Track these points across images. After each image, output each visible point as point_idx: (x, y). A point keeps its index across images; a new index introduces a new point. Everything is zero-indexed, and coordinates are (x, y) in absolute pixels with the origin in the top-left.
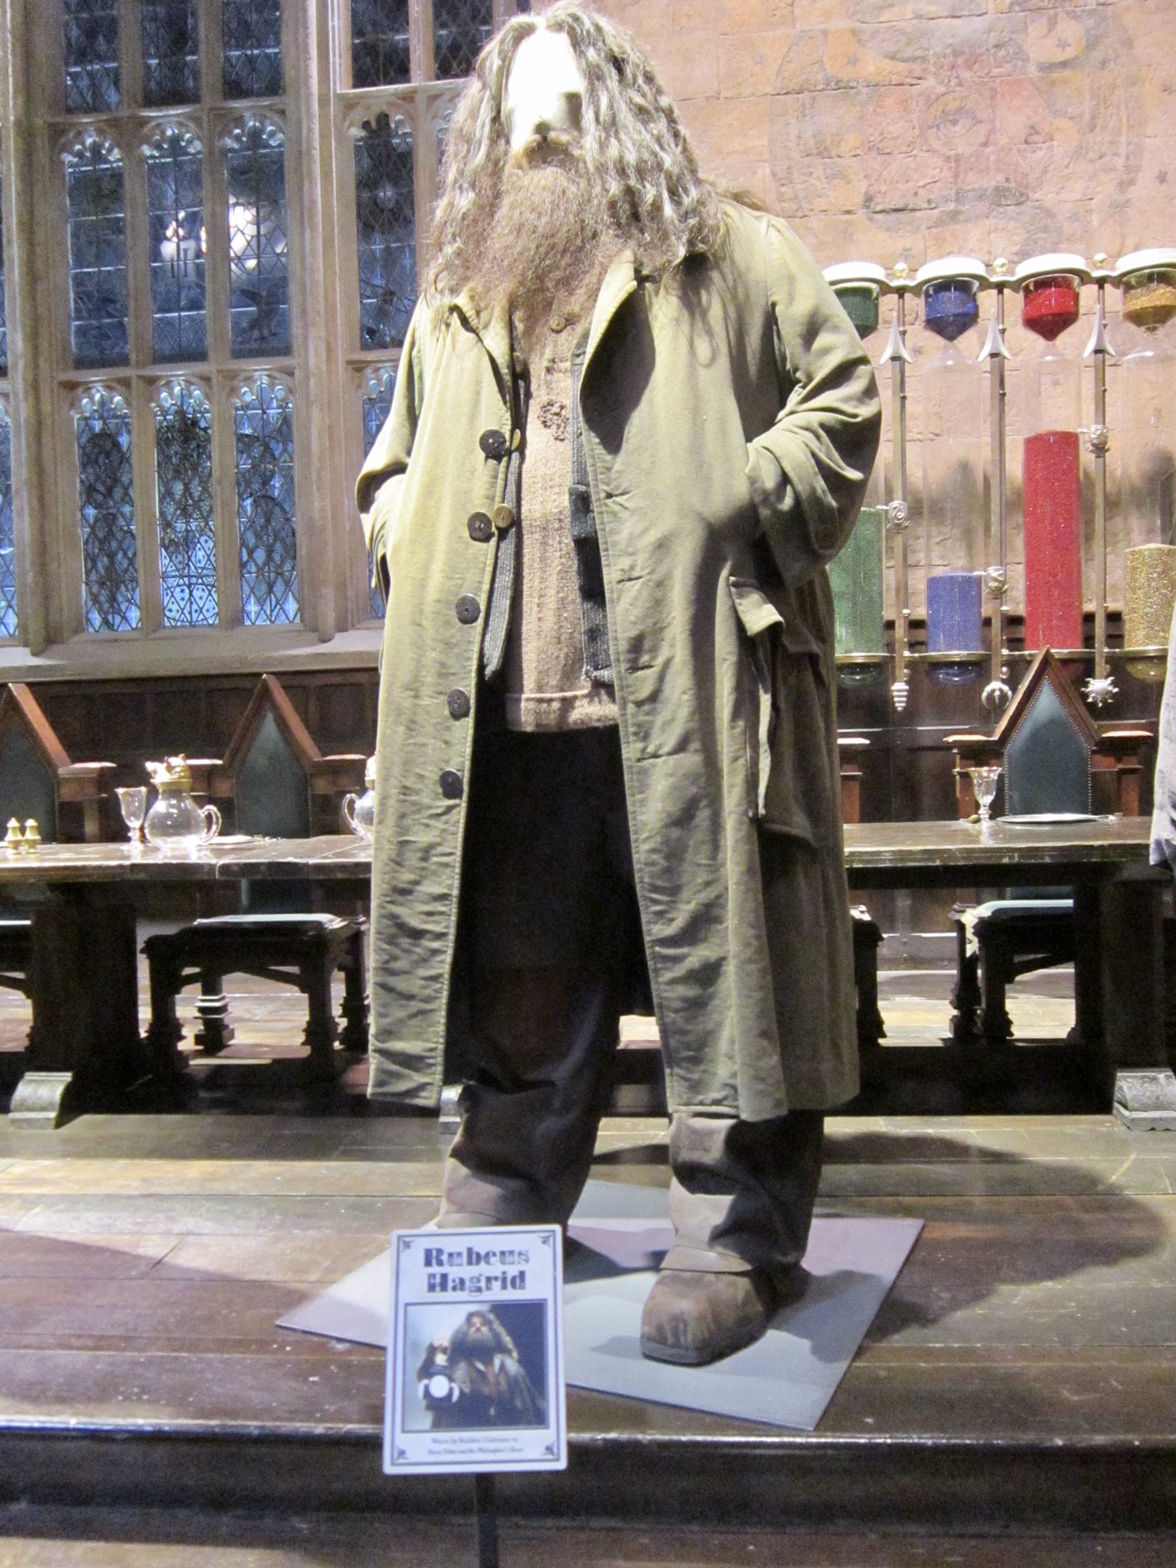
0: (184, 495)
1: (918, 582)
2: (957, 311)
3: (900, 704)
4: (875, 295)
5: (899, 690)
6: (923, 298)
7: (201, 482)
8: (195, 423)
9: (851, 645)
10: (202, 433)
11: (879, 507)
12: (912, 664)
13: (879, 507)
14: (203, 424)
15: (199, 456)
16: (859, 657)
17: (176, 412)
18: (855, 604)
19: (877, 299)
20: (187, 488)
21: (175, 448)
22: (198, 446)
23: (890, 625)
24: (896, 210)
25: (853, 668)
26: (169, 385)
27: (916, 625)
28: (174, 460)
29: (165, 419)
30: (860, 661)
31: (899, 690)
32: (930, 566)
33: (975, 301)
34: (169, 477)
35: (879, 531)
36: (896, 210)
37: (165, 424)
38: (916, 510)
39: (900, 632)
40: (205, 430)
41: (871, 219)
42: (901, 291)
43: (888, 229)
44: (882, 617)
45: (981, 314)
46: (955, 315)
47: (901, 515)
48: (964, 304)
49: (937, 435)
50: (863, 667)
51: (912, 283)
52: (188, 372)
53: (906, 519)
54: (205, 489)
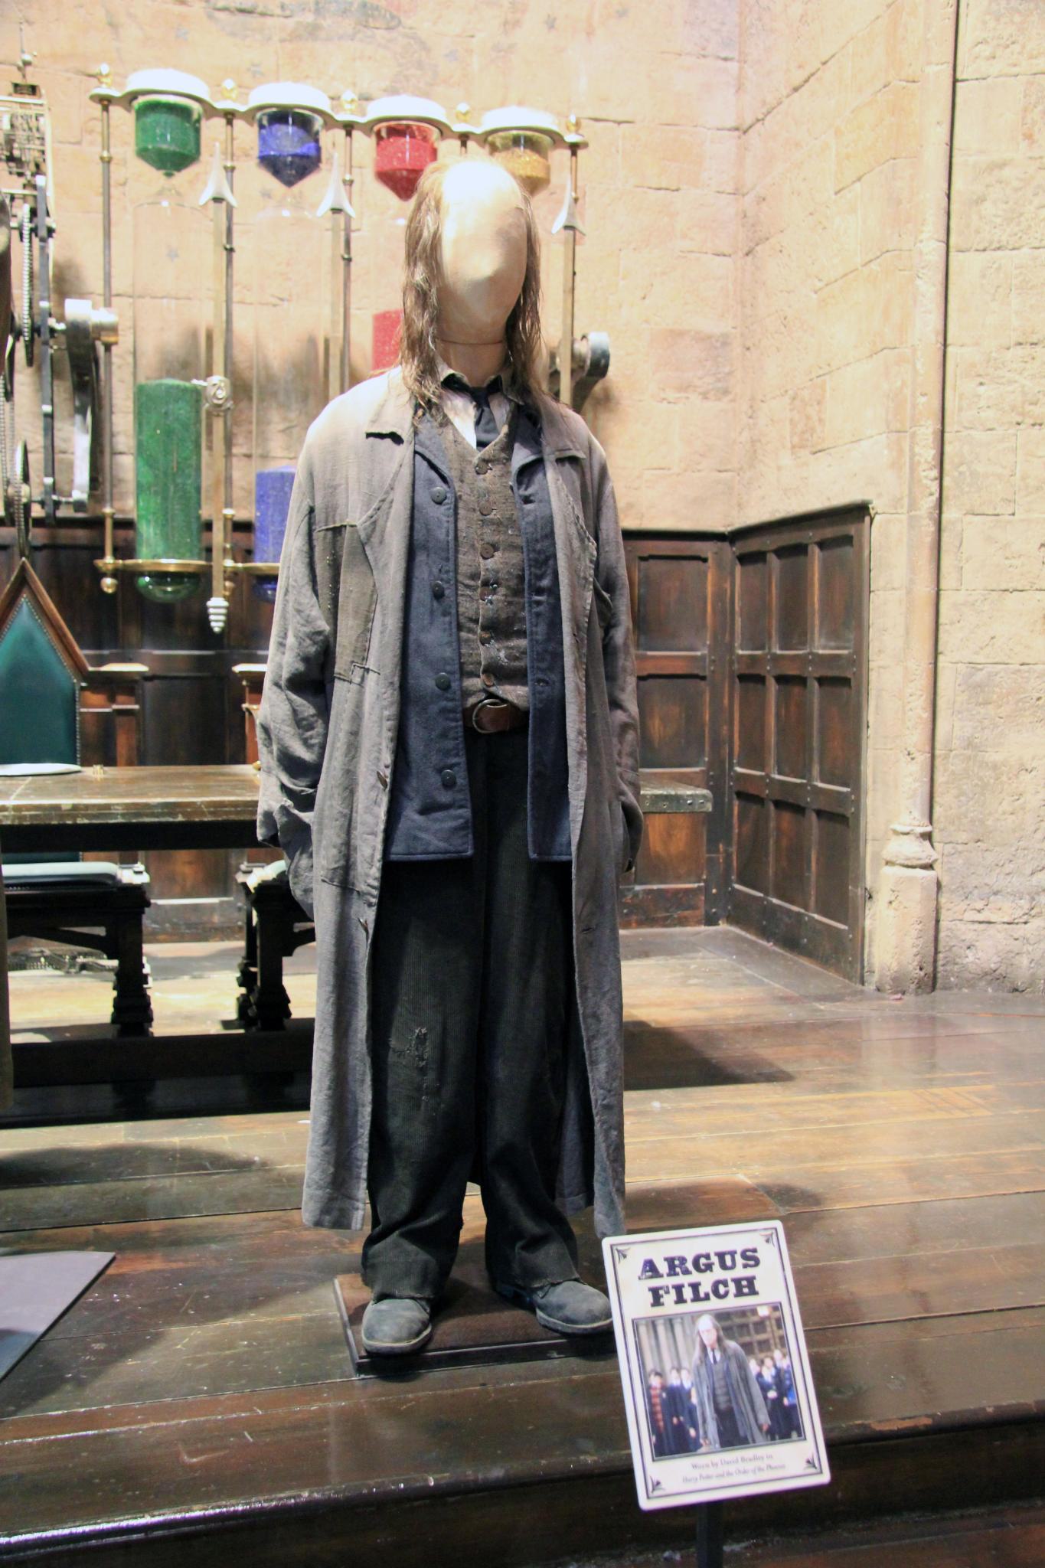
1: (244, 476)
2: (298, 151)
3: (217, 624)
4: (195, 116)
5: (217, 608)
6: (256, 128)
9: (160, 550)
11: (195, 382)
12: (233, 576)
13: (195, 382)
16: (171, 564)
18: (165, 499)
19: (198, 121)
23: (208, 526)
24: (242, 11)
25: (161, 577)
27: (242, 527)
30: (172, 569)
31: (217, 608)
32: (265, 457)
33: (317, 141)
35: (198, 412)
36: (242, 11)
38: (240, 388)
39: (218, 537)
41: (210, 17)
42: (230, 116)
43: (233, 34)
44: (199, 517)
45: (324, 156)
46: (294, 156)
47: (221, 394)
48: (303, 143)
49: (282, 300)
50: (177, 577)
51: (242, 108)
53: (227, 400)
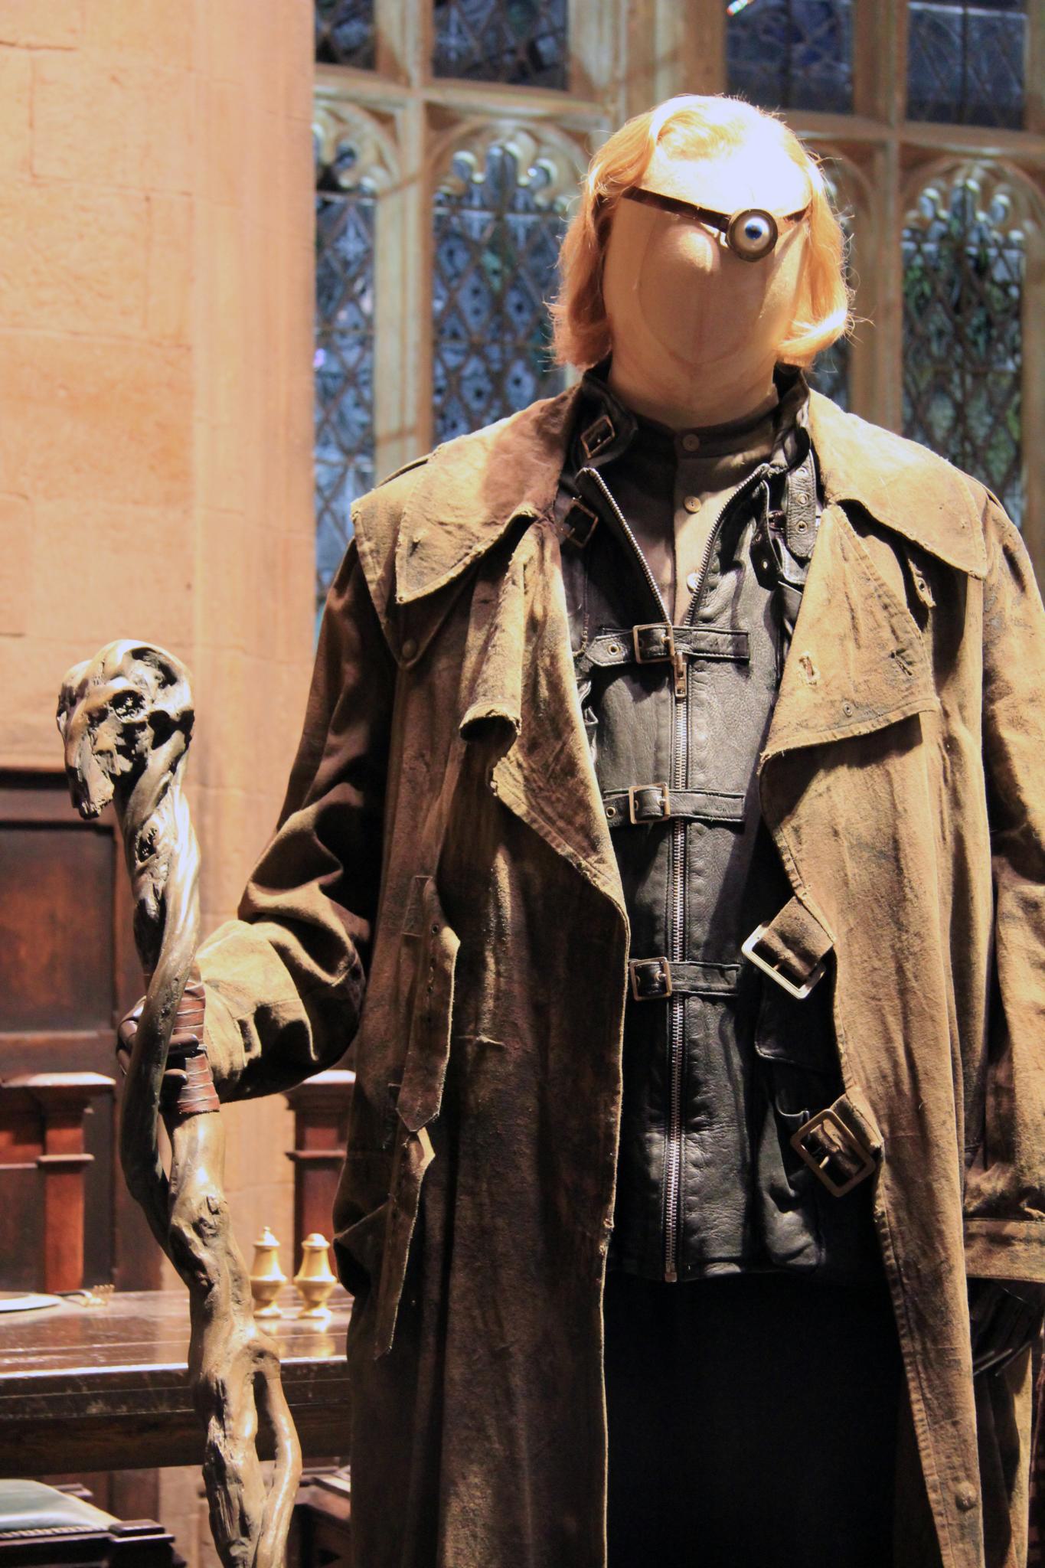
0: (952, 430)
7: (991, 403)
8: (982, 268)
10: (996, 293)
14: (999, 273)
15: (989, 340)
17: (944, 237)
20: (960, 415)
21: (939, 318)
22: (989, 323)
26: (949, 174)
28: (935, 348)
29: (919, 251)
34: (923, 385)
37: (918, 261)
40: (1004, 287)
52: (1011, 150)
54: (999, 421)
